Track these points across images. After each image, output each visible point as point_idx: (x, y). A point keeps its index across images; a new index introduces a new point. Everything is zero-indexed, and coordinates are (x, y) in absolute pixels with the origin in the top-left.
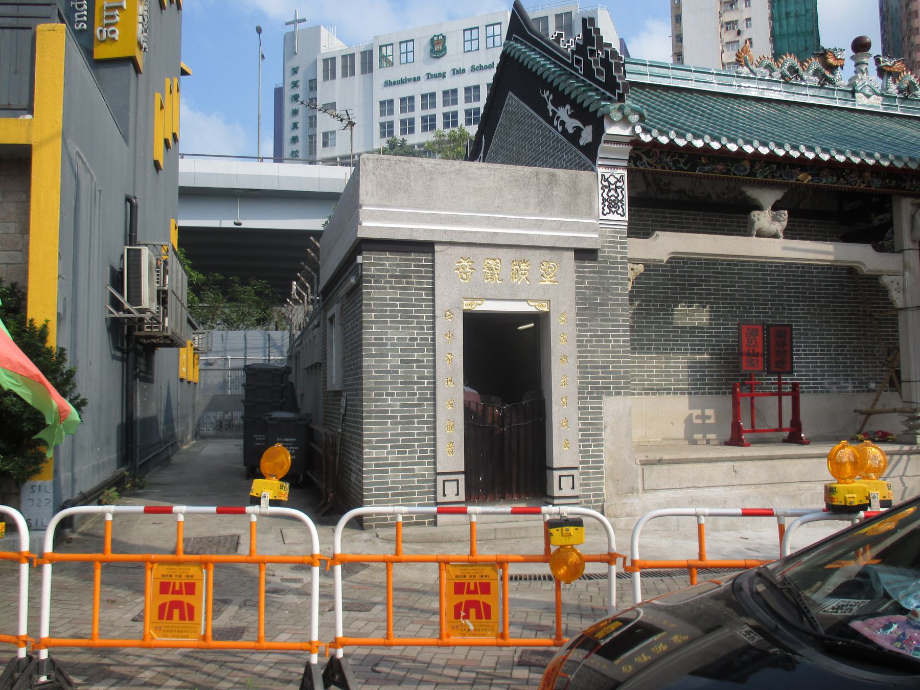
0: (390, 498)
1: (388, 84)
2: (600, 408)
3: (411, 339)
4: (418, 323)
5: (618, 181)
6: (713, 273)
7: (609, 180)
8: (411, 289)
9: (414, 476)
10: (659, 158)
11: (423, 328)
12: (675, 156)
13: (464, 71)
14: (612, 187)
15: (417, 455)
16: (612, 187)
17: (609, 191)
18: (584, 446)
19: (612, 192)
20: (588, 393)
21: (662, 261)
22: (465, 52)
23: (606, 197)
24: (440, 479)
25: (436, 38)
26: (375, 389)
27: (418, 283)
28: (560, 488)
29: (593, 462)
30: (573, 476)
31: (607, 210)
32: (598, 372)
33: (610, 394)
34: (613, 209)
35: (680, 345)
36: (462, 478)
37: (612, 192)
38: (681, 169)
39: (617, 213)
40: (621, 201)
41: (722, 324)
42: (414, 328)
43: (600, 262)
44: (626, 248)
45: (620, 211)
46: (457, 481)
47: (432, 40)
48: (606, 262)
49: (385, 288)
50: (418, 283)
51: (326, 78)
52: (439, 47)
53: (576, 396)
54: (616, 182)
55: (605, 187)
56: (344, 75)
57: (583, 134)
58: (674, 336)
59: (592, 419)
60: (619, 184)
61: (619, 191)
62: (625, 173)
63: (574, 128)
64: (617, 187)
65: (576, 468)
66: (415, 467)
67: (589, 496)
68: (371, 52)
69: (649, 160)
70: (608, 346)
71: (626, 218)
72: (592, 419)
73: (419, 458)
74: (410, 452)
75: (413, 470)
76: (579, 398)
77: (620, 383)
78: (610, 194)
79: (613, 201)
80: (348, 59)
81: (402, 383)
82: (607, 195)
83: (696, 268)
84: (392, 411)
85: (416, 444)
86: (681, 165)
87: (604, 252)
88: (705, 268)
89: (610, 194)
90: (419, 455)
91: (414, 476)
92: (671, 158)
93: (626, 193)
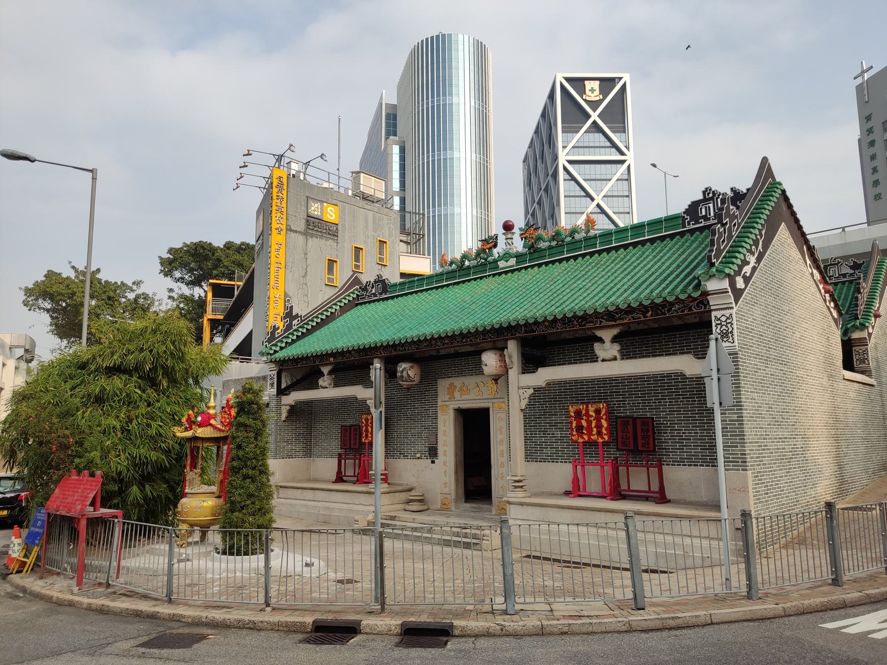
5: (728, 318)
14: (723, 323)
16: (725, 323)
17: (722, 326)
19: (724, 327)
34: (725, 339)
60: (728, 321)
61: (729, 325)
78: (722, 329)
89: (722, 329)
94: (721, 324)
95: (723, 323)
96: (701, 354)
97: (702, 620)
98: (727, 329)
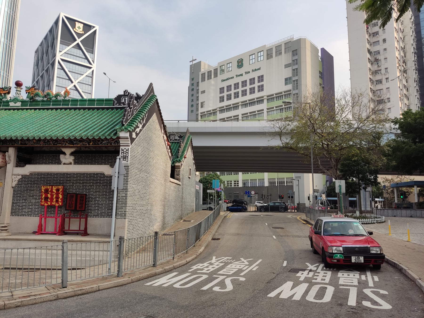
1: (223, 81)
5: (127, 150)
13: (249, 72)
14: (124, 152)
16: (125, 152)
19: (125, 154)
22: (258, 61)
23: (122, 156)
25: (239, 60)
34: (124, 160)
37: (125, 154)
45: (127, 160)
47: (238, 61)
51: (202, 81)
52: (240, 64)
56: (208, 79)
60: (127, 152)
68: (217, 69)
78: (124, 155)
80: (209, 72)
89: (124, 155)
94: (124, 152)
95: (124, 152)
96: (112, 166)
97: (95, 289)
98: (126, 155)
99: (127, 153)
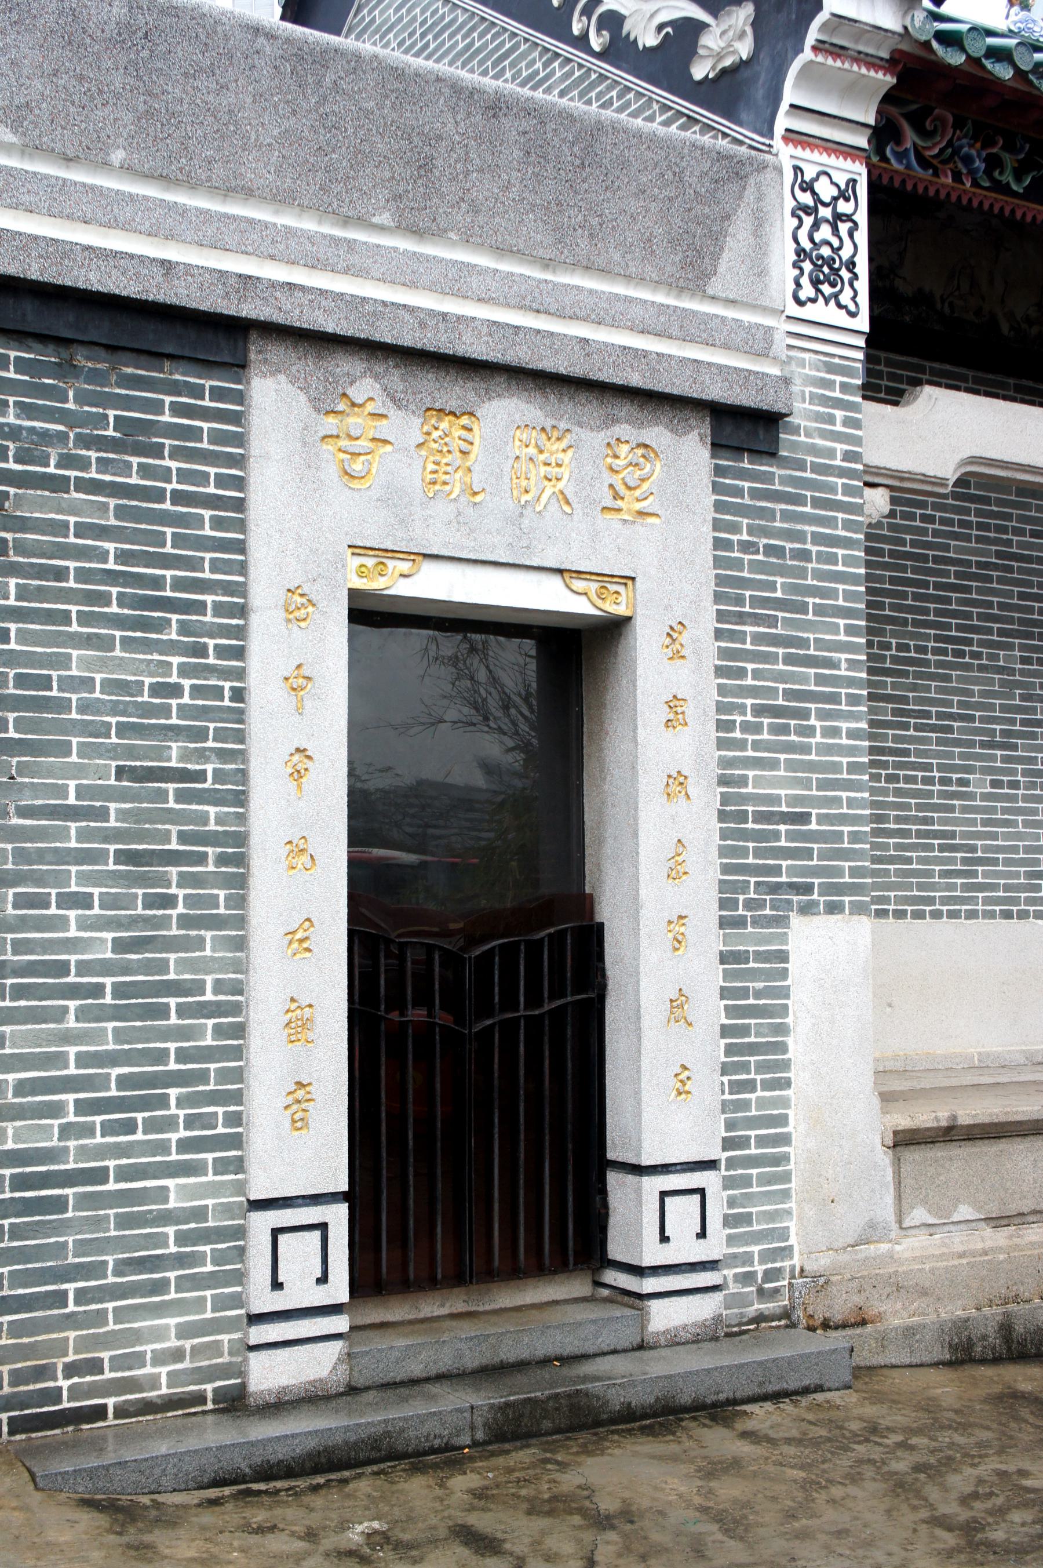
0: (71, 1307)
2: (783, 957)
3: (157, 690)
4: (184, 628)
5: (843, 195)
6: (999, 555)
7: (817, 186)
8: (159, 495)
9: (166, 1218)
10: (950, 143)
11: (201, 651)
12: (993, 144)
15: (174, 1137)
16: (825, 212)
17: (816, 226)
18: (738, 1087)
19: (825, 232)
20: (749, 904)
21: (942, 482)
23: (807, 245)
24: (262, 1222)
26: (18, 879)
27: (184, 476)
28: (664, 1239)
29: (762, 1141)
30: (701, 1192)
31: (807, 291)
32: (776, 835)
33: (807, 909)
34: (826, 289)
35: (914, 766)
36: (338, 1216)
37: (825, 232)
38: (1006, 190)
39: (839, 306)
40: (851, 265)
41: (1019, 709)
42: (172, 648)
43: (785, 463)
44: (856, 424)
46: (323, 1227)
48: (801, 466)
49: (58, 484)
50: (184, 476)
53: (714, 913)
54: (835, 199)
55: (807, 210)
57: (710, 41)
58: (896, 739)
59: (758, 994)
60: (843, 207)
61: (844, 228)
62: (860, 171)
63: (660, 27)
64: (838, 217)
65: (711, 1165)
66: (170, 1183)
67: (747, 1259)
69: (919, 142)
70: (805, 749)
71: (863, 323)
72: (758, 994)
73: (184, 1145)
74: (151, 1126)
75: (162, 1194)
76: (724, 923)
77: (838, 872)
79: (829, 262)
81: (122, 857)
82: (811, 239)
83: (956, 536)
84: (84, 968)
85: (173, 1093)
86: (1008, 178)
87: (796, 430)
88: (979, 539)
89: (818, 237)
90: (183, 1133)
91: (166, 1218)
92: (983, 148)
93: (862, 237)
99: (844, 228)
